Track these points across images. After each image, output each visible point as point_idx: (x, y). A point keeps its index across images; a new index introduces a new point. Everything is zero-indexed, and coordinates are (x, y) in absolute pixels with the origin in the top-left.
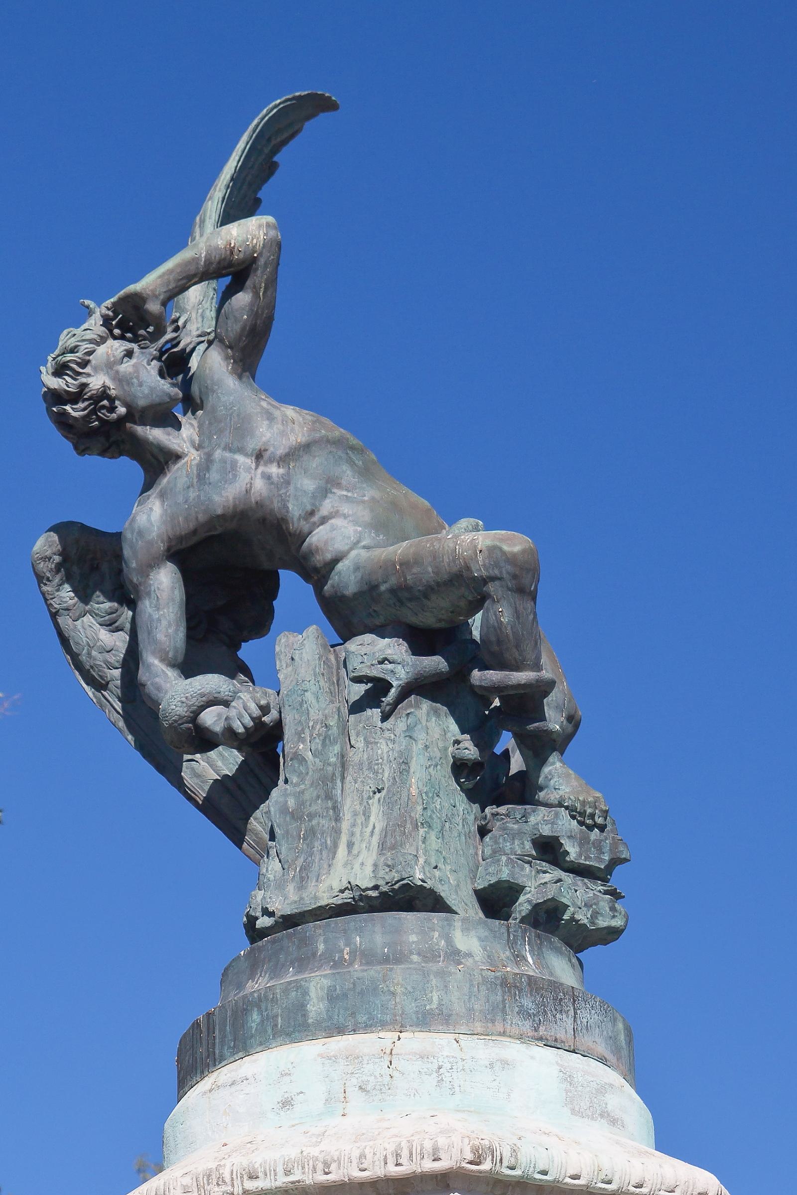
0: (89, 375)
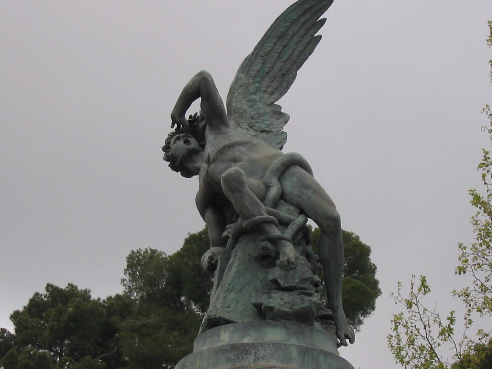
0: (170, 151)
